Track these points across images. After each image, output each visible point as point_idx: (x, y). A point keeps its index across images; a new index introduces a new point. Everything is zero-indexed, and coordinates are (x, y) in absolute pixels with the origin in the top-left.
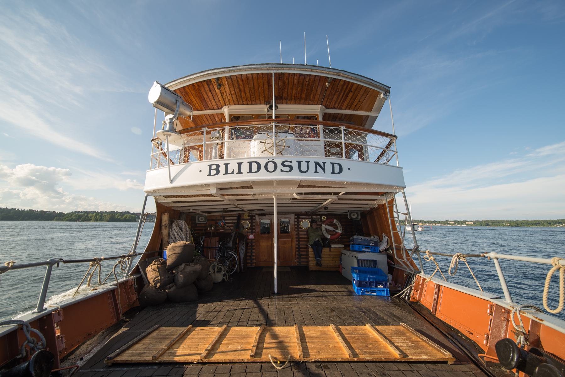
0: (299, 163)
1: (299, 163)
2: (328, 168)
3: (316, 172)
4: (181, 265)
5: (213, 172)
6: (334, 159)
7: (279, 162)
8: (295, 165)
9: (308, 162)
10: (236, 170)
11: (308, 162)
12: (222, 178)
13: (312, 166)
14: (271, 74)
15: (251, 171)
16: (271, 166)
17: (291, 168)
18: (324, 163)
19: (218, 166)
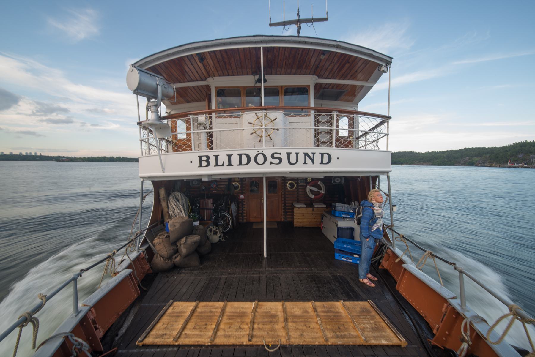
0: (289, 154)
1: (289, 154)
2: (318, 158)
3: (305, 163)
4: (182, 238)
5: (204, 163)
6: (324, 149)
7: (268, 154)
8: (284, 157)
9: (297, 154)
10: (226, 163)
11: (297, 154)
12: (212, 170)
13: (301, 157)
14: (260, 48)
15: (241, 164)
16: (260, 159)
17: (281, 160)
18: (314, 154)
19: (208, 157)
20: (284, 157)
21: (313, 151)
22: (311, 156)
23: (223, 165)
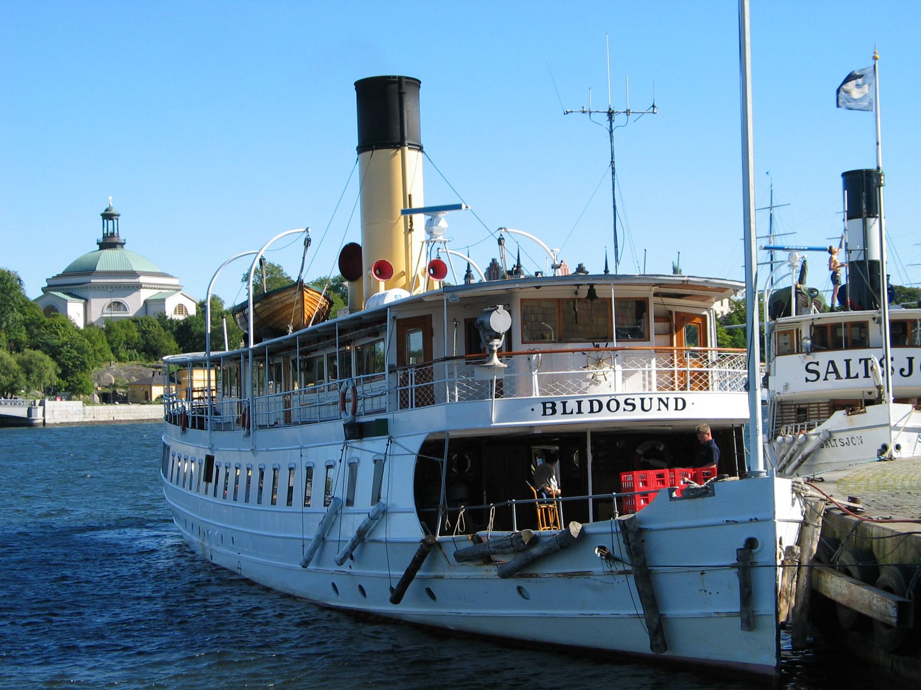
0: (642, 400)
1: (642, 400)
5: (549, 411)
7: (621, 400)
8: (638, 403)
9: (651, 399)
11: (651, 399)
12: (558, 419)
13: (655, 402)
15: (592, 411)
16: (613, 405)
19: (554, 404)
20: (638, 403)
21: (667, 396)
22: (665, 401)
23: (572, 413)
